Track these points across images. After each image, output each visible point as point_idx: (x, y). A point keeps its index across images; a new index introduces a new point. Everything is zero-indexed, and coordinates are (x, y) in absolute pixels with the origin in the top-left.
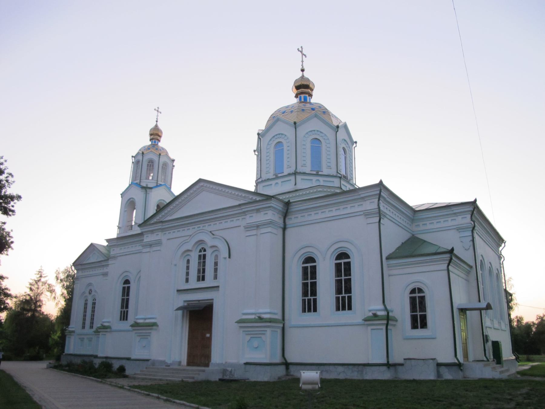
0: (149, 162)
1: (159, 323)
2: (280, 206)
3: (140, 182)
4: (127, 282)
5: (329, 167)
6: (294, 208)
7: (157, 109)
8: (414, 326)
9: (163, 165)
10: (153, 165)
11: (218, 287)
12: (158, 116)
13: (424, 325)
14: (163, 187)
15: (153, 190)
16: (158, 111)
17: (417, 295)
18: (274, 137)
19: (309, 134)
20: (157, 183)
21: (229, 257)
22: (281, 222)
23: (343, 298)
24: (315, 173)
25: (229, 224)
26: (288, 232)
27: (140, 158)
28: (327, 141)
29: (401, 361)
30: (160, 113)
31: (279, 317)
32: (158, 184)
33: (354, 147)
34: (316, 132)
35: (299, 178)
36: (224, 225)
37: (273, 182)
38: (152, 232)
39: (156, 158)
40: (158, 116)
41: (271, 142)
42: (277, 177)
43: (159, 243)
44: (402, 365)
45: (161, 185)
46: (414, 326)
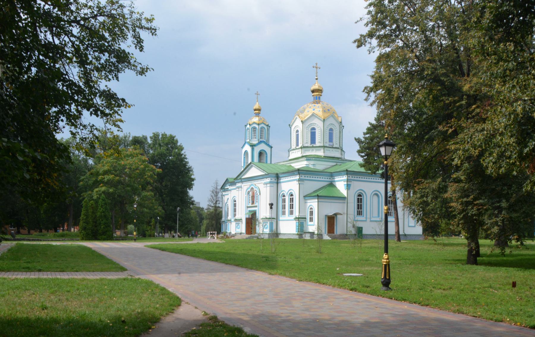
4: (235, 201)
5: (319, 142)
12: (257, 97)
13: (312, 221)
16: (257, 94)
17: (311, 210)
22: (276, 181)
24: (311, 146)
25: (260, 182)
26: (279, 184)
36: (258, 182)
37: (294, 151)
38: (239, 182)
40: (257, 97)
42: (296, 149)
43: (241, 187)
46: (310, 221)
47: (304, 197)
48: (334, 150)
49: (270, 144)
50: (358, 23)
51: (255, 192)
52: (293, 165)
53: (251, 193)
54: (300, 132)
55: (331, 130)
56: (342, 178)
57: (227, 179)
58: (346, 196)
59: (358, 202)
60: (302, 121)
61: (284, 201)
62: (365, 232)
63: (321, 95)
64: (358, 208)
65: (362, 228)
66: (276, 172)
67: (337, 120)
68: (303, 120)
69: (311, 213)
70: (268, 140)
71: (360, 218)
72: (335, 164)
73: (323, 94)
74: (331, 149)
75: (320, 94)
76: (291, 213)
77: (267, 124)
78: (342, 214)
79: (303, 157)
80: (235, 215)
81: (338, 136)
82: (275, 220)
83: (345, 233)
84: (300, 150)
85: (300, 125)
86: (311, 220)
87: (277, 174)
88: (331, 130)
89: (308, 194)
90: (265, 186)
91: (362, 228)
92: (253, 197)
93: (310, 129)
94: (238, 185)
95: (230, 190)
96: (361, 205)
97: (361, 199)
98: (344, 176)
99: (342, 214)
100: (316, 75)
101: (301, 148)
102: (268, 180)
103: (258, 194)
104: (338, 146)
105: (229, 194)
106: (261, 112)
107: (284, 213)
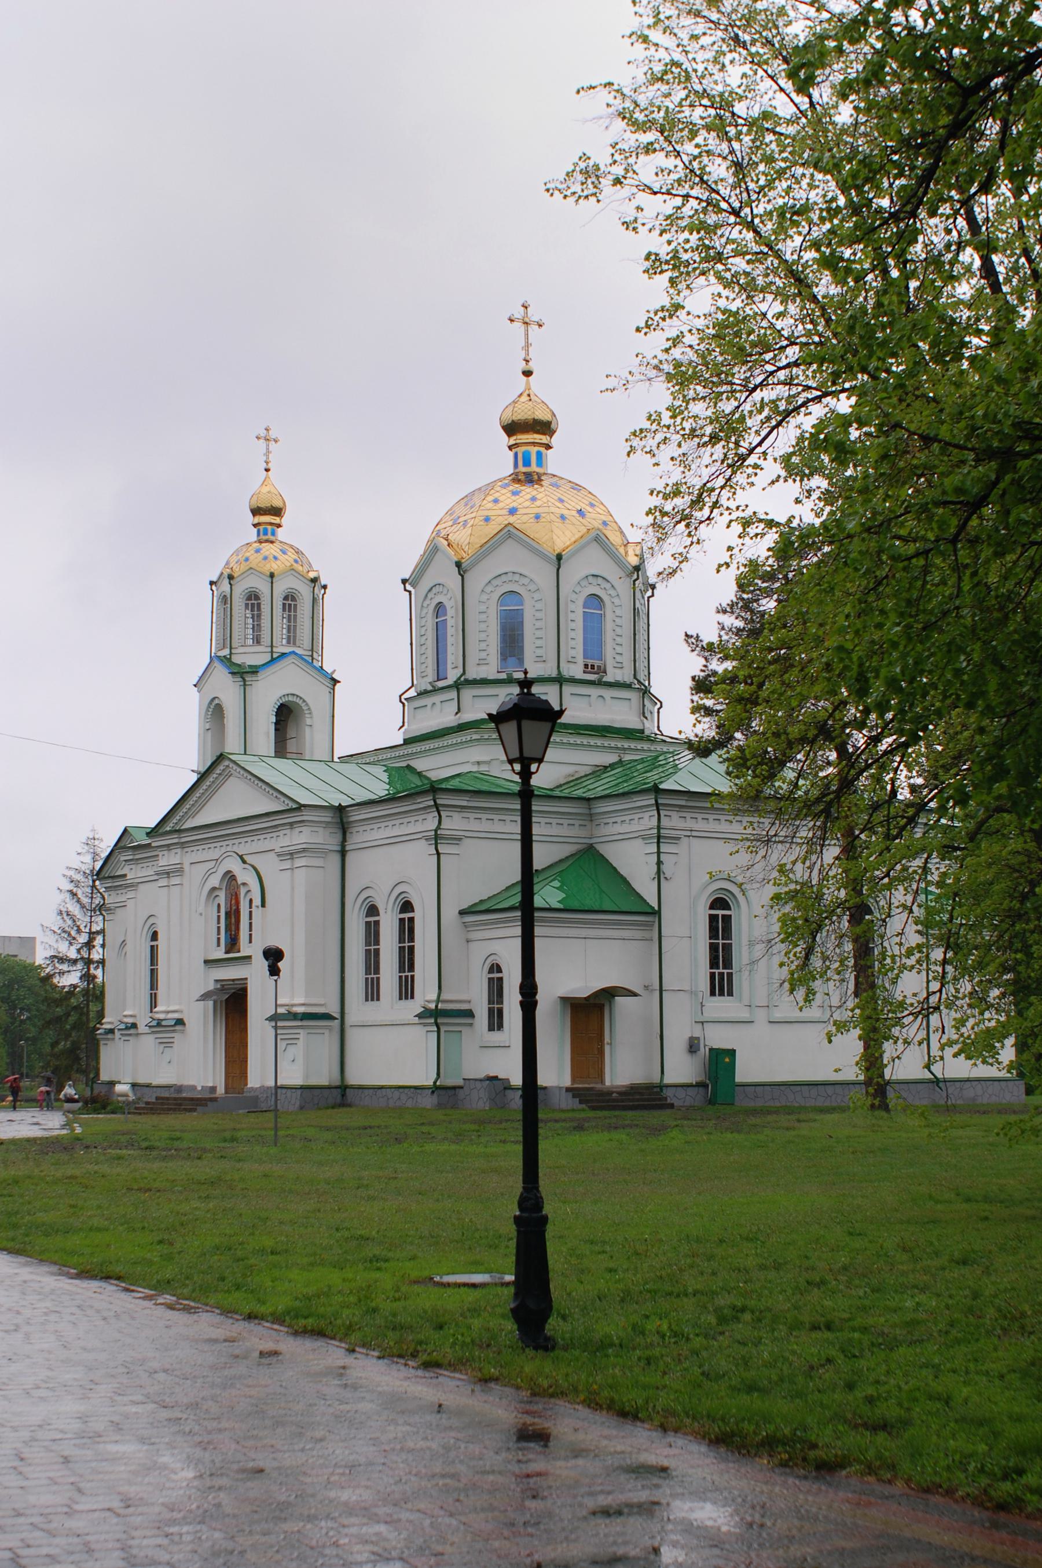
0: (249, 598)
1: (186, 1021)
2: (327, 817)
3: (231, 654)
5: (541, 660)
6: (356, 816)
7: (263, 433)
8: (491, 1029)
9: (286, 598)
10: (259, 605)
11: (250, 957)
12: (268, 452)
13: (500, 1026)
14: (291, 659)
15: (261, 675)
18: (430, 590)
19: (495, 582)
20: (272, 652)
21: (263, 905)
23: (406, 977)
24: (504, 676)
26: (350, 858)
27: (225, 586)
28: (537, 596)
29: (461, 1083)
30: (276, 441)
31: (334, 1010)
32: (275, 656)
33: (634, 581)
34: (510, 577)
35: (467, 693)
39: (263, 588)
40: (268, 452)
41: (427, 602)
42: (435, 690)
43: (179, 871)
44: (461, 1087)
45: (283, 655)
46: (491, 1029)
47: (462, 913)
48: (608, 693)
49: (328, 668)
50: (610, 128)
51: (243, 891)
52: (420, 765)
53: (222, 899)
54: (450, 612)
55: (595, 600)
56: (634, 827)
57: (125, 830)
58: (656, 908)
59: (713, 932)
60: (458, 565)
61: (372, 933)
62: (746, 1071)
63: (548, 447)
64: (714, 963)
65: (732, 1053)
66: (336, 800)
67: (618, 561)
68: (466, 558)
69: (496, 989)
70: (315, 646)
71: (719, 1006)
72: (611, 758)
73: (555, 441)
74: (594, 692)
75: (544, 439)
76: (407, 990)
77: (312, 575)
78: (635, 995)
79: (461, 728)
80: (153, 1002)
81: (627, 630)
82: (336, 1023)
83: (656, 1080)
84: (453, 694)
85: (453, 581)
86: (496, 1021)
87: (341, 809)
88: (595, 600)
89: (475, 905)
90: (287, 865)
91: (732, 1053)
92: (233, 916)
93: (496, 596)
94: (167, 860)
95: (133, 886)
96: (728, 948)
97: (727, 919)
98: (646, 815)
99: (635, 995)
100: (523, 354)
101: (458, 686)
102: (301, 837)
103: (257, 901)
104: (625, 675)
105: (130, 904)
106: (285, 520)
107: (372, 992)
